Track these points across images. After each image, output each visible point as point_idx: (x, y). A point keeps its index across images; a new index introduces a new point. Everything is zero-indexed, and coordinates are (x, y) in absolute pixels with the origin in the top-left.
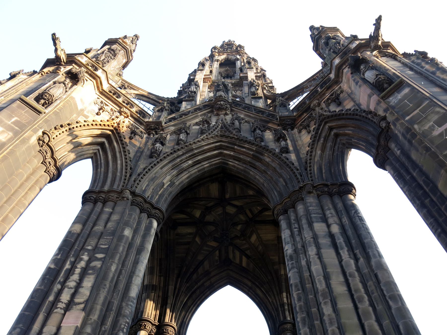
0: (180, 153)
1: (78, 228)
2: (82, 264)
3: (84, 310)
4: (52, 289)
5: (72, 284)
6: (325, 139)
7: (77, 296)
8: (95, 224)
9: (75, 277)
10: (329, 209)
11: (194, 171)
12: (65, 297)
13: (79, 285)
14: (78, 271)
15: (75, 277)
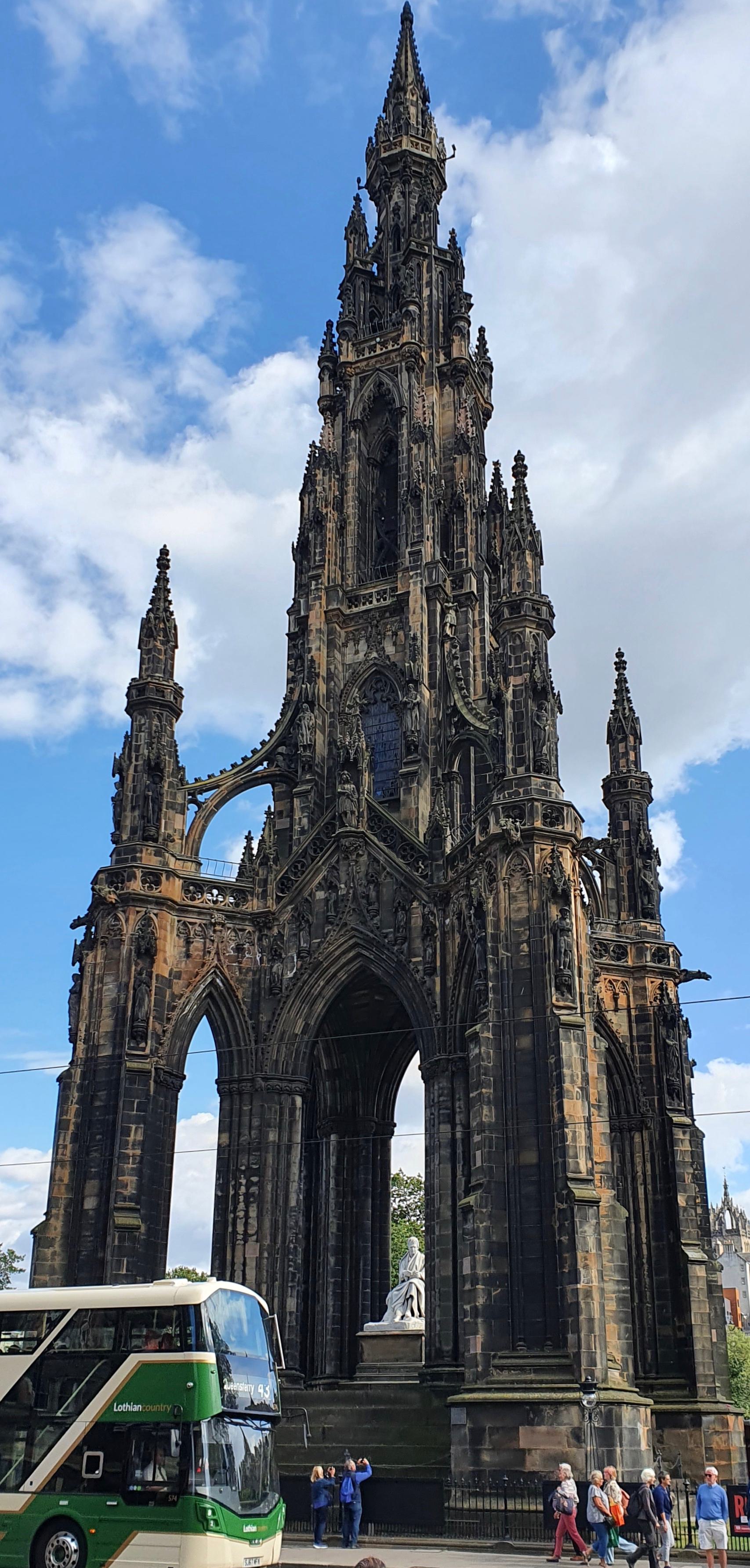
0: (305, 977)
1: (225, 1136)
2: (243, 1189)
3: (257, 1241)
4: (228, 1220)
5: (241, 1214)
6: (470, 966)
7: (249, 1228)
8: (239, 1134)
9: (242, 1206)
10: (459, 1100)
11: (329, 992)
12: (240, 1229)
13: (247, 1216)
14: (241, 1198)
15: (242, 1206)
